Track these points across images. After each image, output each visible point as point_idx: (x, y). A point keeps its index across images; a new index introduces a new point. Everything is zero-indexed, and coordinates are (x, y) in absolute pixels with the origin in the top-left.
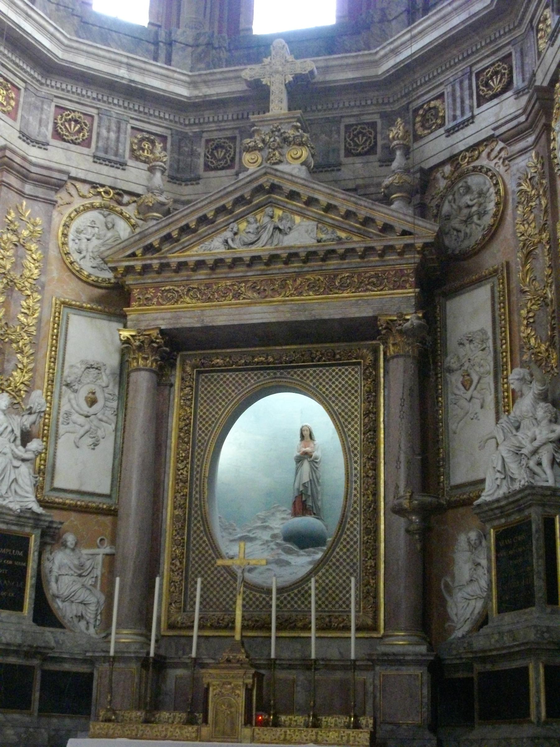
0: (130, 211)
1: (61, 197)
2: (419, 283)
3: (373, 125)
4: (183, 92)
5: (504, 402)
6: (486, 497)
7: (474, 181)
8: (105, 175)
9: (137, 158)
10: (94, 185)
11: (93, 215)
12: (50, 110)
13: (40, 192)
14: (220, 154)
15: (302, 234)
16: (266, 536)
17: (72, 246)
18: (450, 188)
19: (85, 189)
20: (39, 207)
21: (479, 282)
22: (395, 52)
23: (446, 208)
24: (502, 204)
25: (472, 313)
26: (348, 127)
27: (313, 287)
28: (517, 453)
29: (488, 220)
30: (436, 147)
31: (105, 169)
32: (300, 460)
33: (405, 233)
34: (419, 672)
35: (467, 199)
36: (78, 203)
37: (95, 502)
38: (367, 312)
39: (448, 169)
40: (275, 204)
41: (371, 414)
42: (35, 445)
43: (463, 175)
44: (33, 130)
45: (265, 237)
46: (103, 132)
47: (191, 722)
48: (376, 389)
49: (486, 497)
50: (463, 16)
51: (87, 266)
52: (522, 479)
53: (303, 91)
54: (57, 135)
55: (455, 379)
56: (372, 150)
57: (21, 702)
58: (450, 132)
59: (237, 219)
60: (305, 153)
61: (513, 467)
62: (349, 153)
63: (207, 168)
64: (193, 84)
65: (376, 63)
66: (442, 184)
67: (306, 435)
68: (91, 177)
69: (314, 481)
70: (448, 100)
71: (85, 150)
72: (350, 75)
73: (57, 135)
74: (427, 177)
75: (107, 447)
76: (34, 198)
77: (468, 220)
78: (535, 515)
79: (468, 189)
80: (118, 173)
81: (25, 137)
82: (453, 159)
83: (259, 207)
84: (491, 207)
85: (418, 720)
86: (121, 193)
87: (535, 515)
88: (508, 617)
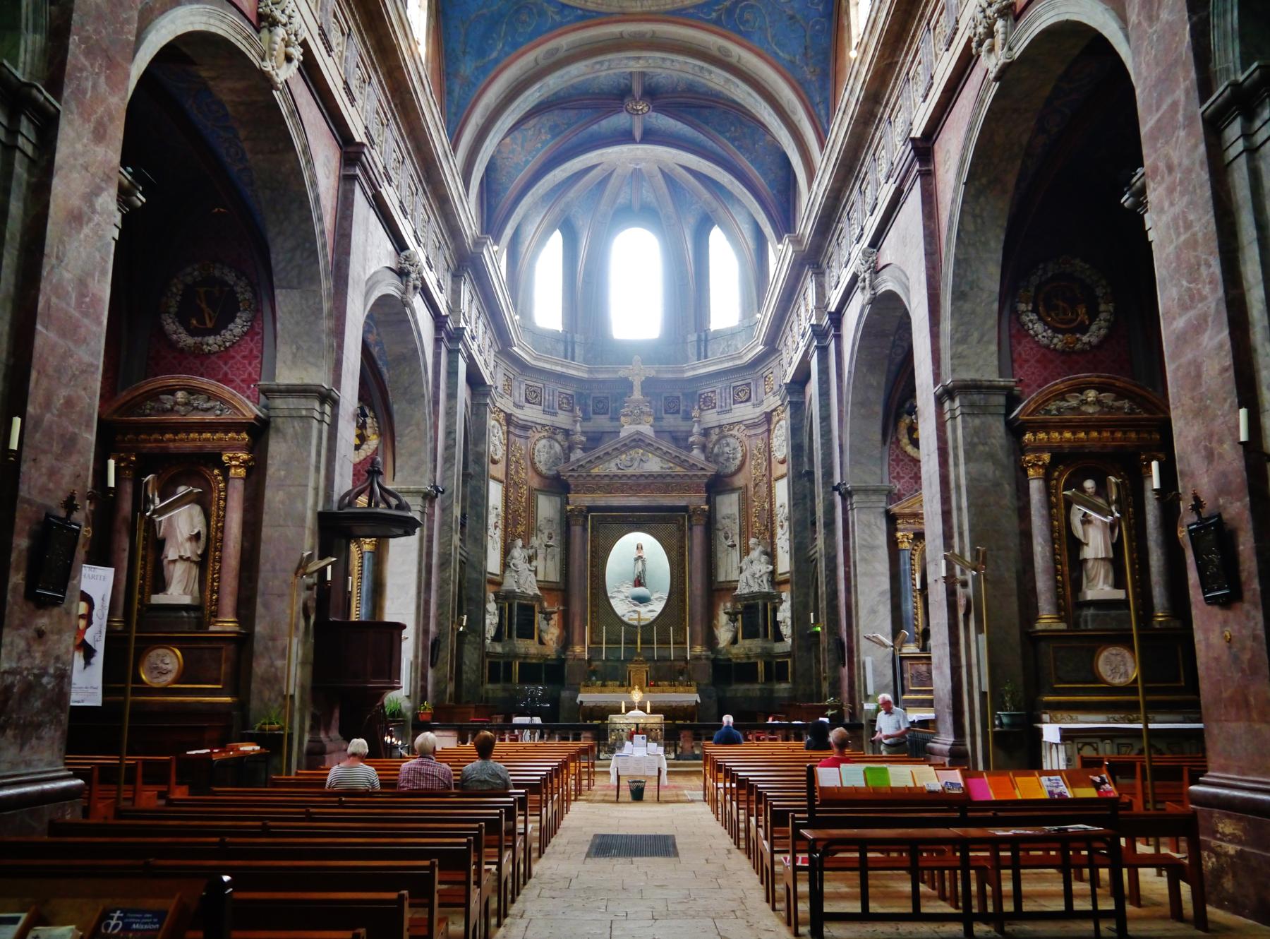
0: (560, 437)
1: (530, 433)
2: (708, 491)
3: (678, 398)
4: (585, 375)
5: (746, 551)
6: (738, 592)
7: (731, 440)
8: (547, 420)
9: (561, 408)
10: (544, 426)
11: (544, 442)
12: (523, 387)
13: (522, 433)
14: (601, 406)
15: (654, 465)
16: (621, 596)
17: (536, 459)
18: (718, 441)
19: (539, 427)
20: (522, 440)
21: (733, 490)
22: (693, 369)
23: (716, 450)
24: (744, 456)
25: (728, 505)
26: (666, 398)
27: (659, 490)
28: (753, 575)
29: (737, 462)
30: (711, 418)
31: (548, 417)
32: (636, 560)
33: (702, 469)
34: (709, 663)
35: (727, 449)
36: (538, 436)
37: (554, 586)
38: (683, 503)
39: (717, 430)
40: (640, 447)
41: (682, 547)
42: (534, 563)
43: (725, 437)
44: (517, 400)
45: (636, 464)
46: (546, 396)
47: (622, 685)
48: (683, 537)
49: (738, 592)
50: (731, 364)
51: (542, 468)
52: (755, 589)
53: (650, 385)
54: (527, 401)
55: (721, 535)
56: (678, 412)
57: (536, 681)
58: (719, 413)
59: (622, 453)
60: (651, 419)
61: (751, 582)
62: (666, 412)
63: (595, 413)
64: (590, 371)
65: (683, 372)
66: (714, 438)
67: (639, 548)
68: (543, 422)
69: (644, 570)
70: (718, 397)
71: (540, 408)
72: (670, 376)
73: (527, 401)
74: (706, 432)
75: (558, 558)
76: (520, 436)
77: (728, 459)
78: (760, 602)
79: (728, 445)
80: (554, 418)
81: (516, 405)
82: (720, 426)
83: (634, 447)
84: (739, 455)
85: (706, 681)
86: (556, 428)
87: (760, 602)
88: (748, 642)
